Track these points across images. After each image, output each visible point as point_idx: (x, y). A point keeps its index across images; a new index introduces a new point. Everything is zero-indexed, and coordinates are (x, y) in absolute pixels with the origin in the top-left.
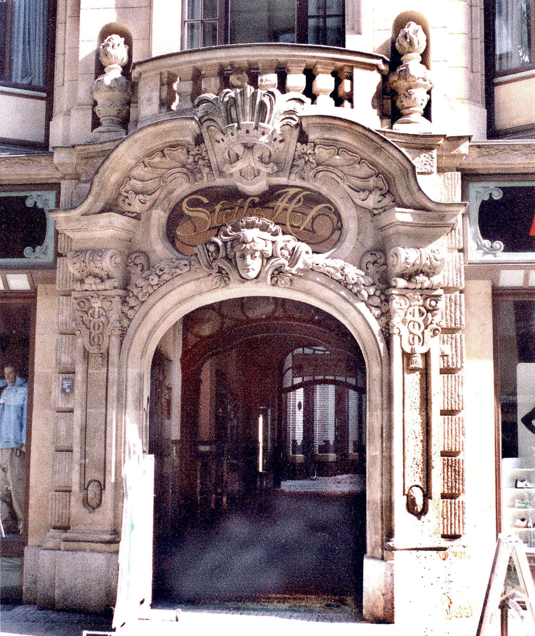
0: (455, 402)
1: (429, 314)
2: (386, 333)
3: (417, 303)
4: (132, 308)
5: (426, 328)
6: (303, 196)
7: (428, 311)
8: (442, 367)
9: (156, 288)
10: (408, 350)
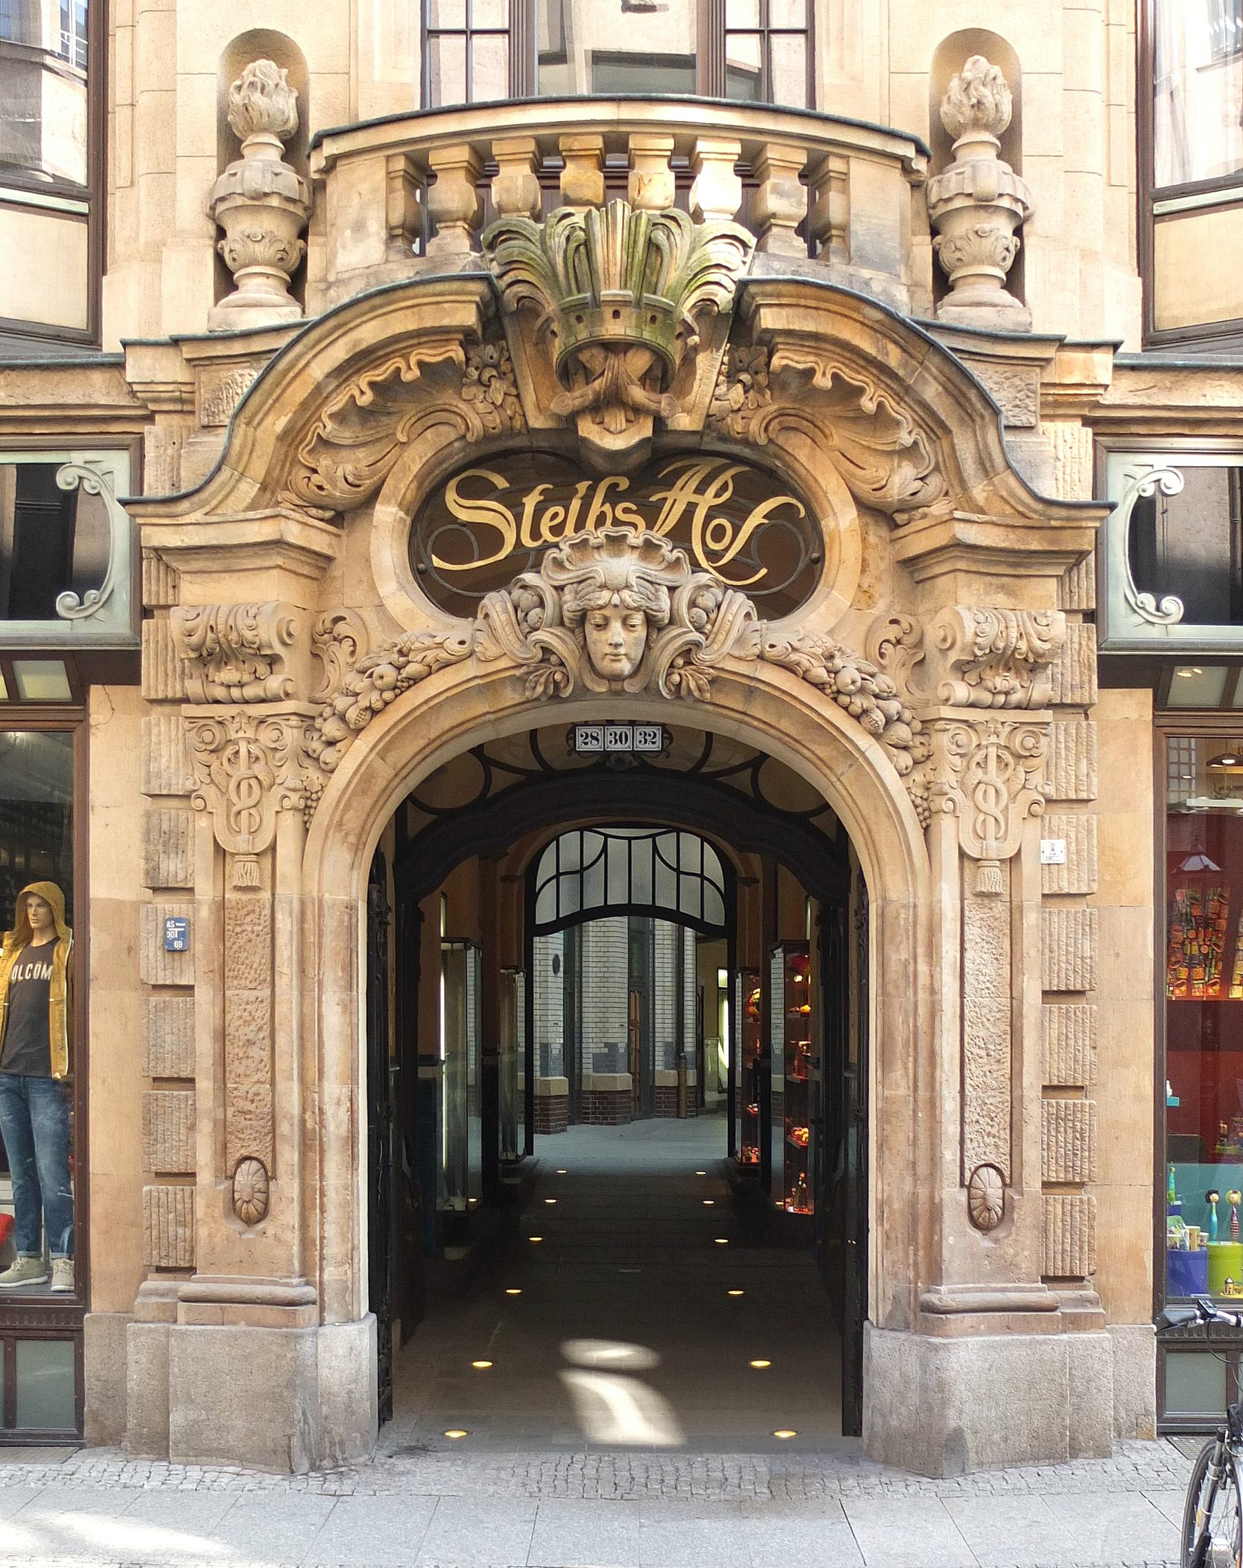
4: (331, 743)
6: (732, 477)
9: (388, 695)
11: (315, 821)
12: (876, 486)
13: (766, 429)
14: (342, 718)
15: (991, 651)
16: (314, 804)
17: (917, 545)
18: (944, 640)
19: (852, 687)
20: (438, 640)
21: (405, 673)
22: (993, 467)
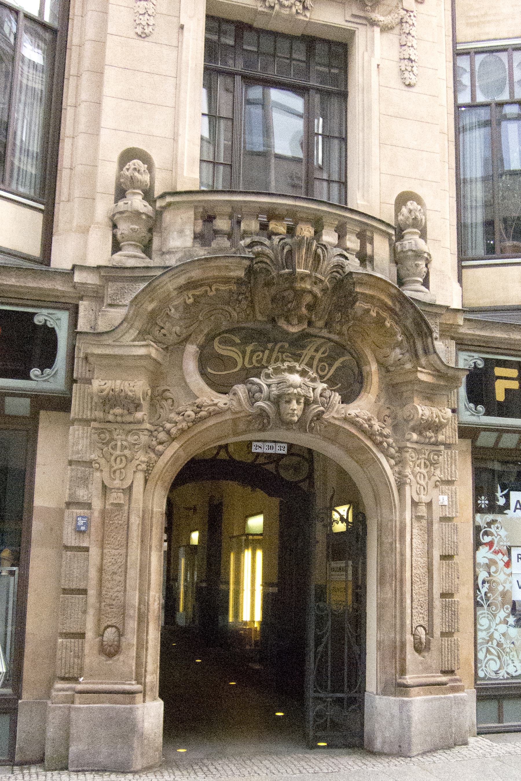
3: (423, 456)
5: (429, 479)
7: (432, 464)
9: (190, 424)
10: (416, 499)
14: (168, 432)
17: (399, 379)
20: (215, 402)
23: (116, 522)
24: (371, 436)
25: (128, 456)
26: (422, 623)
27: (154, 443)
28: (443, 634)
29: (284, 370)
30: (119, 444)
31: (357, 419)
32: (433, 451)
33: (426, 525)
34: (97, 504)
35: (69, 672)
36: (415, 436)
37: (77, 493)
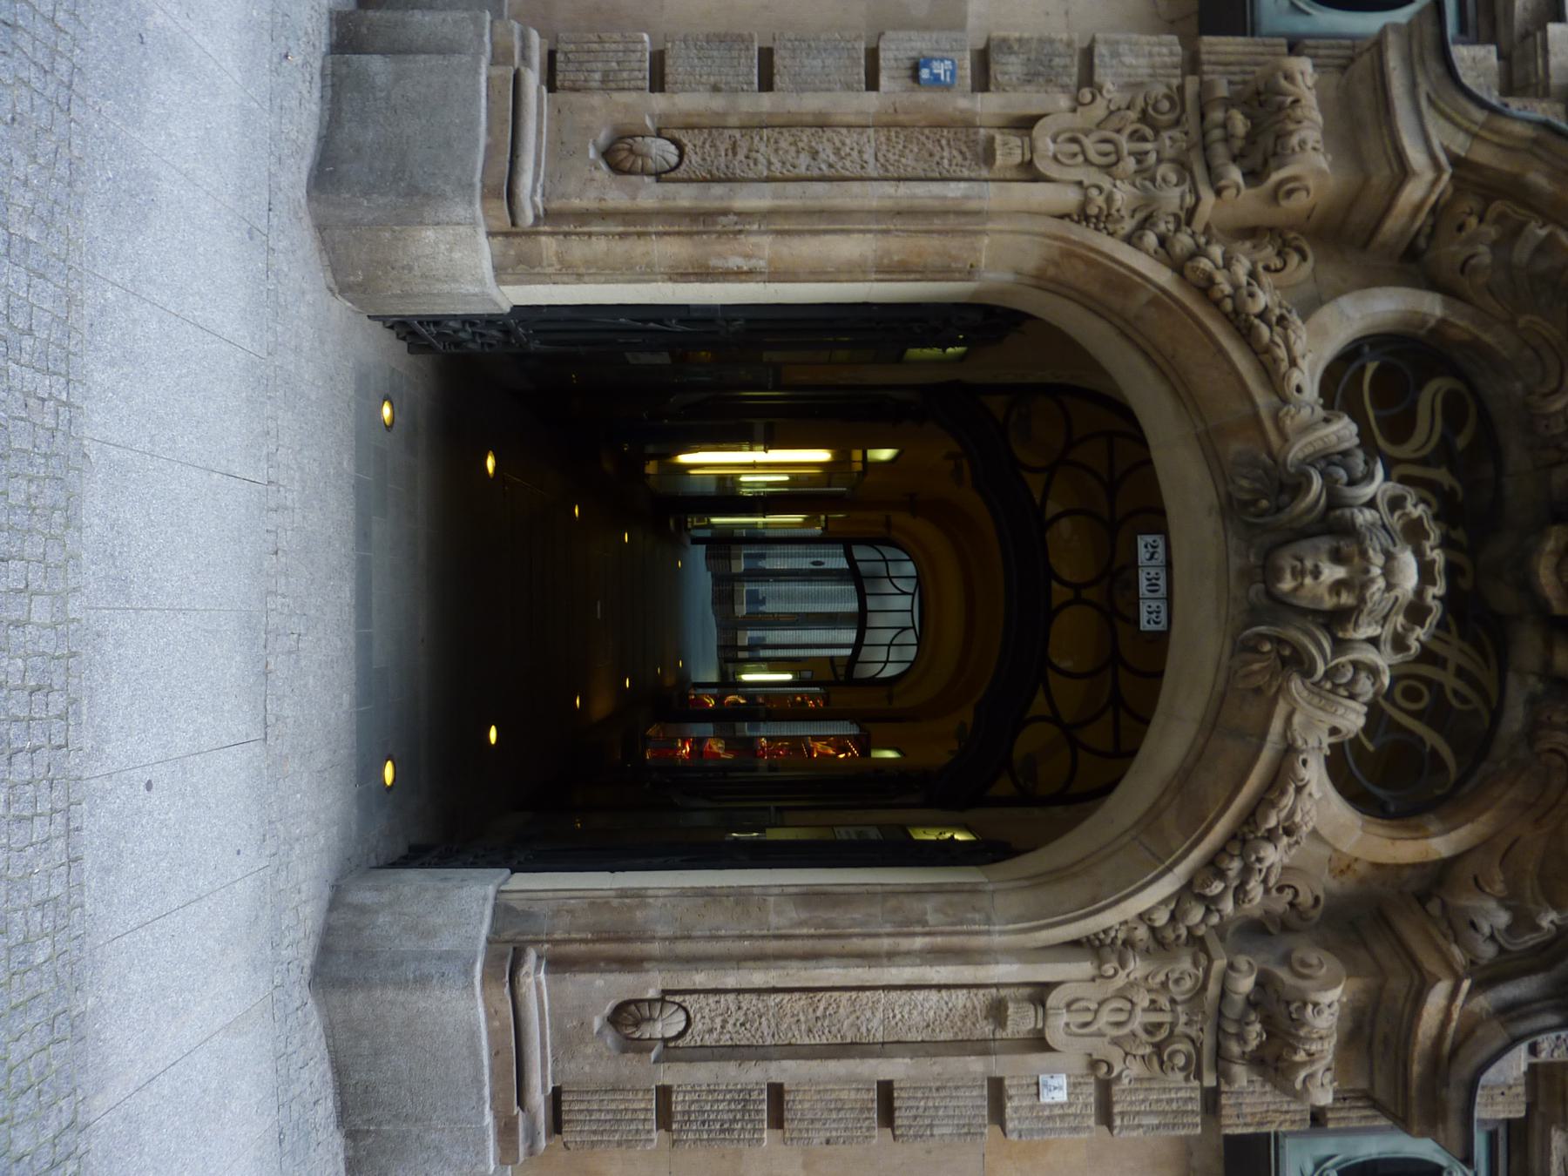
0: (915, 1117)
1: (1148, 1050)
2: (1100, 940)
3: (1183, 1019)
5: (1116, 1042)
7: (1158, 1048)
8: (1007, 1082)
9: (1228, 305)
10: (1055, 999)
11: (1074, 226)
12: (1480, 880)
13: (1552, 751)
15: (1293, 1020)
16: (1092, 226)
18: (1304, 964)
19: (1253, 858)
20: (1300, 361)
21: (1257, 321)
22: (1512, 1020)
23: (946, 154)
24: (1244, 837)
25: (1121, 165)
26: (698, 1026)
27: (1162, 227)
28: (664, 1093)
29: (1419, 553)
30: (1148, 146)
31: (1291, 789)
32: (1199, 1052)
33: (977, 1035)
34: (989, 106)
35: (568, 61)
36: (1245, 984)
37: (1013, 59)
